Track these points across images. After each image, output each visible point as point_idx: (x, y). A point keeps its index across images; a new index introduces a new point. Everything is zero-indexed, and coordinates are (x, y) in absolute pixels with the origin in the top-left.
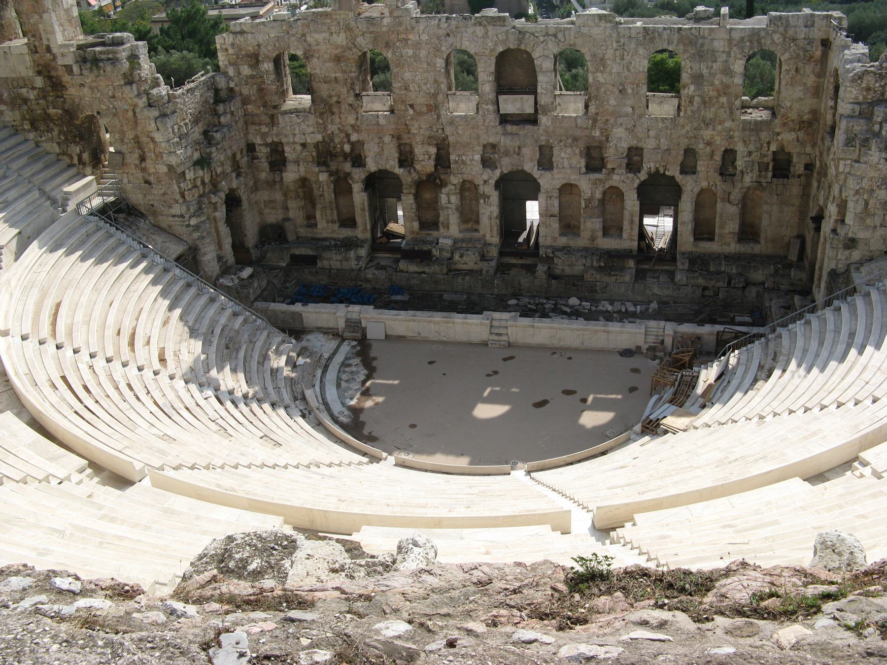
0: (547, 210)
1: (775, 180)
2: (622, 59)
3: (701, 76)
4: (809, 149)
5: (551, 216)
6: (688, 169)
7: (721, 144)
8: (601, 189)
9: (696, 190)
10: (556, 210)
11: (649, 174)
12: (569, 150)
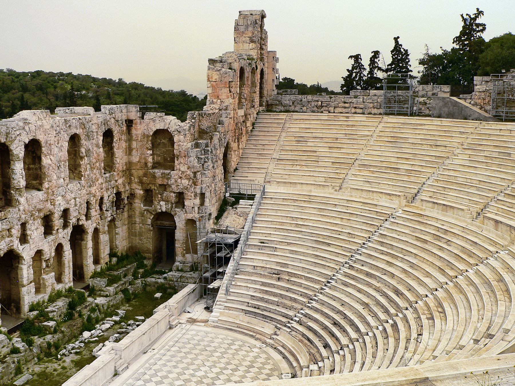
0: (28, 280)
1: (118, 211)
2: (58, 144)
3: (89, 150)
4: (127, 188)
5: (31, 282)
6: (88, 216)
7: (99, 195)
8: (54, 248)
9: (93, 229)
10: (32, 277)
11: (74, 227)
12: (36, 222)
